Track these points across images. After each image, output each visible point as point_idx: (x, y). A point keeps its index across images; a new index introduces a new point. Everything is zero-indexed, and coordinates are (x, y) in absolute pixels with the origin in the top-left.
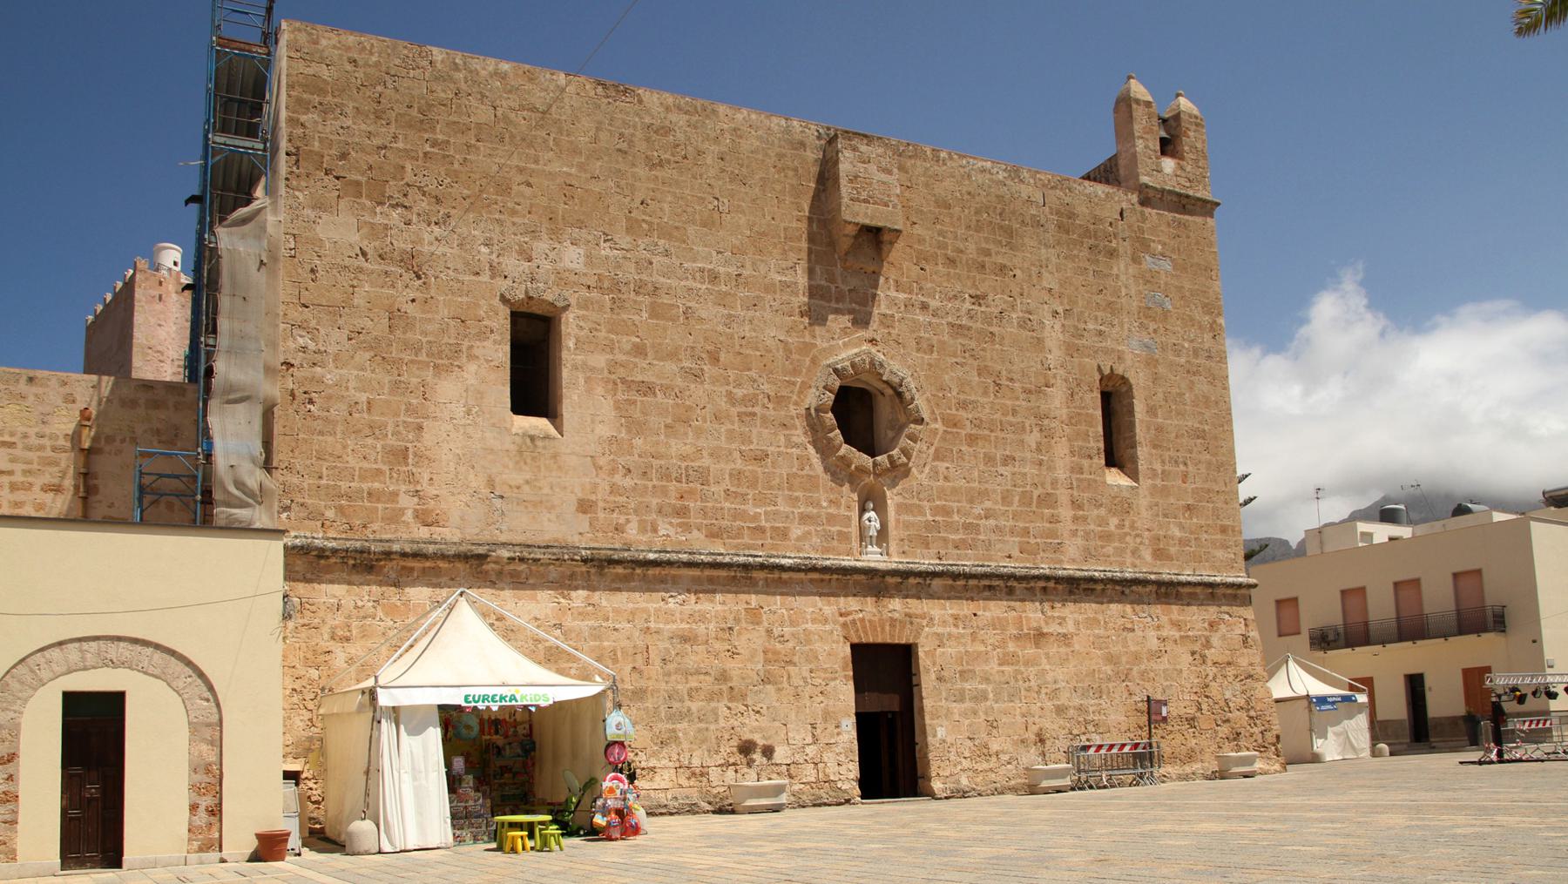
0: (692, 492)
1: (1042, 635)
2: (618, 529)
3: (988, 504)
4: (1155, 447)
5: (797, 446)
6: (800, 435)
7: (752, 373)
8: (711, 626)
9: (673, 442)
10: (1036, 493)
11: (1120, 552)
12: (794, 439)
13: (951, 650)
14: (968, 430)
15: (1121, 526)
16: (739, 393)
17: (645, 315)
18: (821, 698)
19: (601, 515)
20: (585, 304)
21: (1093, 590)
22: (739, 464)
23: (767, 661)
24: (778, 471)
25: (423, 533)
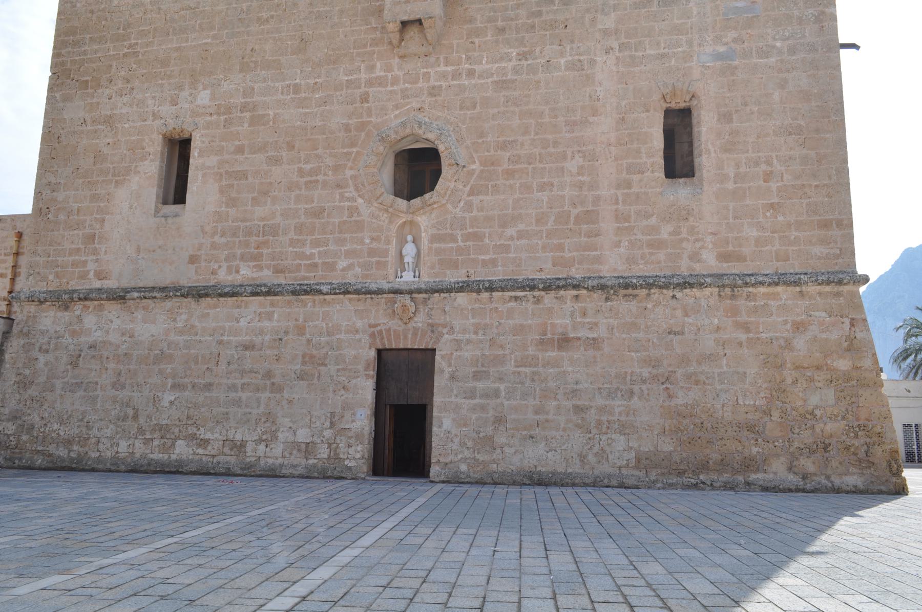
0: (266, 243)
2: (214, 273)
3: (521, 227)
4: (726, 151)
5: (349, 199)
6: (350, 192)
7: (320, 151)
8: (267, 338)
9: (257, 208)
10: (575, 212)
12: (347, 195)
14: (505, 166)
16: (308, 167)
17: (246, 125)
18: (343, 392)
19: (203, 264)
20: (208, 126)
21: (635, 296)
23: (304, 363)
24: (332, 220)
25: (97, 284)
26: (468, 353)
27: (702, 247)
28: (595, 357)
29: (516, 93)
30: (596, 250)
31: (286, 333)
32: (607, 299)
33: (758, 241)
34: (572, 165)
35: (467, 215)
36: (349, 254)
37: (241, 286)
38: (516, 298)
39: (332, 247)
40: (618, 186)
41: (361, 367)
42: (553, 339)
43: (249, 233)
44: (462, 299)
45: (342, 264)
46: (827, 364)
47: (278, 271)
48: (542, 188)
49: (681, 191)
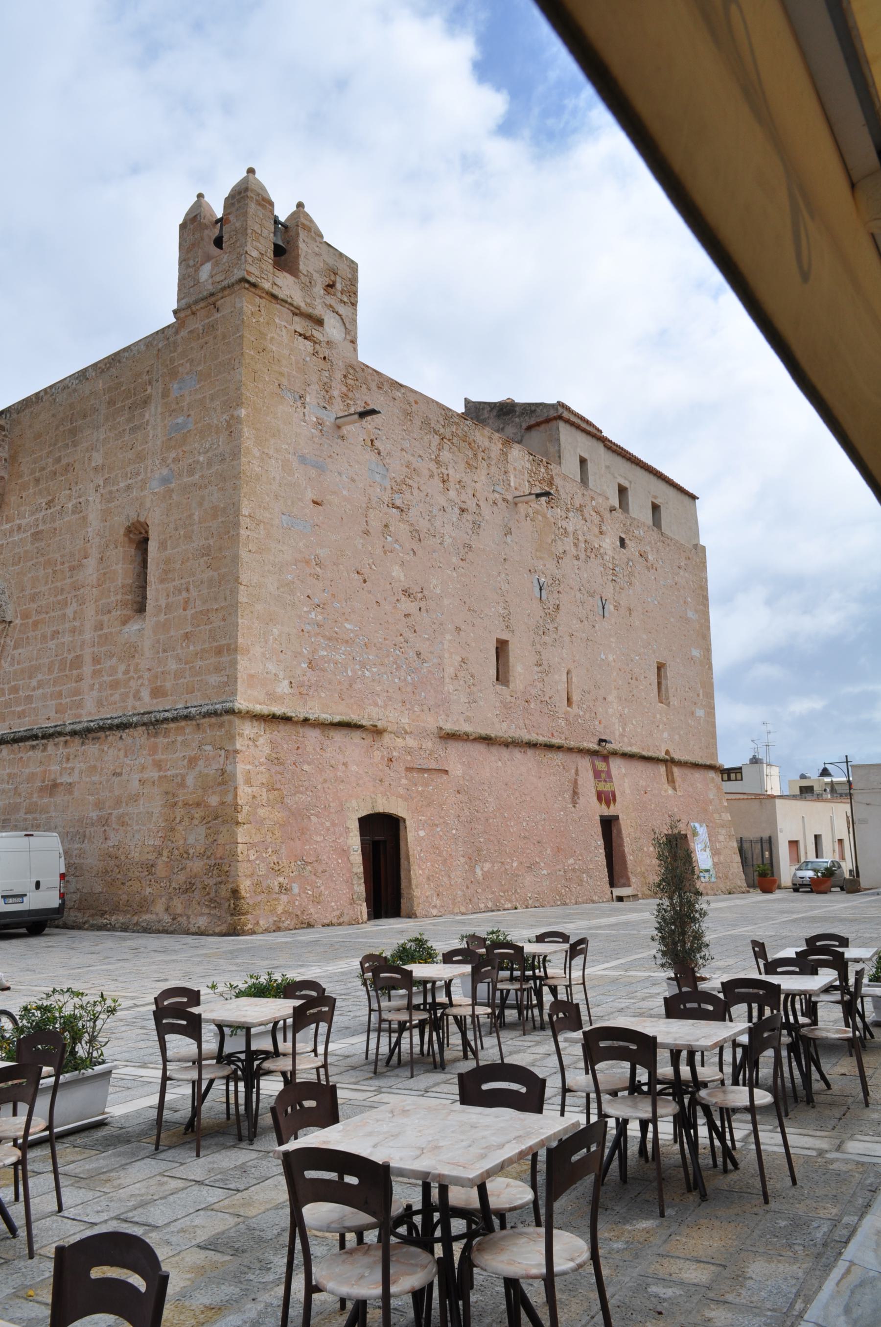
3: (40, 677)
11: (124, 697)
15: (127, 672)
27: (142, 685)
32: (83, 744)
34: (69, 611)
46: (204, 801)
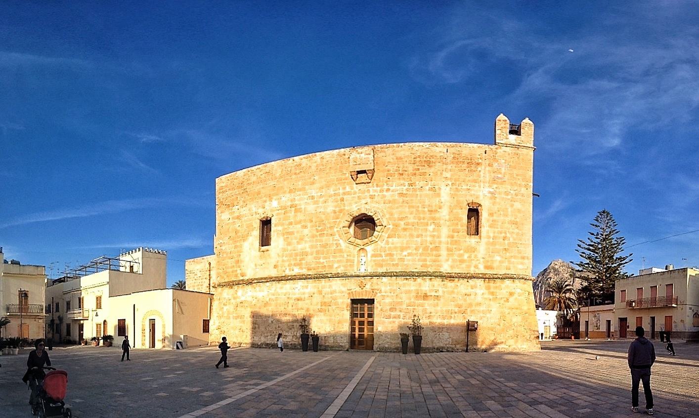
1: (427, 296)
3: (410, 251)
10: (431, 246)
13: (388, 300)
15: (469, 257)
22: (319, 249)
26: (388, 300)
28: (437, 303)
29: (407, 199)
30: (439, 261)
31: (314, 294)
32: (442, 281)
33: (500, 262)
35: (387, 246)
36: (339, 261)
37: (295, 276)
38: (406, 279)
39: (332, 259)
40: (449, 237)
41: (345, 306)
42: (421, 296)
43: (296, 255)
44: (385, 279)
45: (336, 265)
47: (309, 269)
48: (418, 236)
49: (474, 240)
